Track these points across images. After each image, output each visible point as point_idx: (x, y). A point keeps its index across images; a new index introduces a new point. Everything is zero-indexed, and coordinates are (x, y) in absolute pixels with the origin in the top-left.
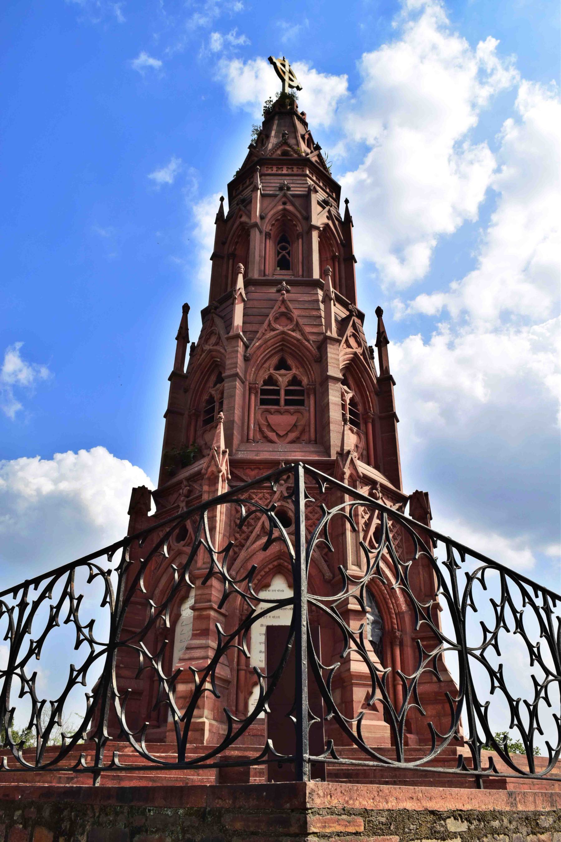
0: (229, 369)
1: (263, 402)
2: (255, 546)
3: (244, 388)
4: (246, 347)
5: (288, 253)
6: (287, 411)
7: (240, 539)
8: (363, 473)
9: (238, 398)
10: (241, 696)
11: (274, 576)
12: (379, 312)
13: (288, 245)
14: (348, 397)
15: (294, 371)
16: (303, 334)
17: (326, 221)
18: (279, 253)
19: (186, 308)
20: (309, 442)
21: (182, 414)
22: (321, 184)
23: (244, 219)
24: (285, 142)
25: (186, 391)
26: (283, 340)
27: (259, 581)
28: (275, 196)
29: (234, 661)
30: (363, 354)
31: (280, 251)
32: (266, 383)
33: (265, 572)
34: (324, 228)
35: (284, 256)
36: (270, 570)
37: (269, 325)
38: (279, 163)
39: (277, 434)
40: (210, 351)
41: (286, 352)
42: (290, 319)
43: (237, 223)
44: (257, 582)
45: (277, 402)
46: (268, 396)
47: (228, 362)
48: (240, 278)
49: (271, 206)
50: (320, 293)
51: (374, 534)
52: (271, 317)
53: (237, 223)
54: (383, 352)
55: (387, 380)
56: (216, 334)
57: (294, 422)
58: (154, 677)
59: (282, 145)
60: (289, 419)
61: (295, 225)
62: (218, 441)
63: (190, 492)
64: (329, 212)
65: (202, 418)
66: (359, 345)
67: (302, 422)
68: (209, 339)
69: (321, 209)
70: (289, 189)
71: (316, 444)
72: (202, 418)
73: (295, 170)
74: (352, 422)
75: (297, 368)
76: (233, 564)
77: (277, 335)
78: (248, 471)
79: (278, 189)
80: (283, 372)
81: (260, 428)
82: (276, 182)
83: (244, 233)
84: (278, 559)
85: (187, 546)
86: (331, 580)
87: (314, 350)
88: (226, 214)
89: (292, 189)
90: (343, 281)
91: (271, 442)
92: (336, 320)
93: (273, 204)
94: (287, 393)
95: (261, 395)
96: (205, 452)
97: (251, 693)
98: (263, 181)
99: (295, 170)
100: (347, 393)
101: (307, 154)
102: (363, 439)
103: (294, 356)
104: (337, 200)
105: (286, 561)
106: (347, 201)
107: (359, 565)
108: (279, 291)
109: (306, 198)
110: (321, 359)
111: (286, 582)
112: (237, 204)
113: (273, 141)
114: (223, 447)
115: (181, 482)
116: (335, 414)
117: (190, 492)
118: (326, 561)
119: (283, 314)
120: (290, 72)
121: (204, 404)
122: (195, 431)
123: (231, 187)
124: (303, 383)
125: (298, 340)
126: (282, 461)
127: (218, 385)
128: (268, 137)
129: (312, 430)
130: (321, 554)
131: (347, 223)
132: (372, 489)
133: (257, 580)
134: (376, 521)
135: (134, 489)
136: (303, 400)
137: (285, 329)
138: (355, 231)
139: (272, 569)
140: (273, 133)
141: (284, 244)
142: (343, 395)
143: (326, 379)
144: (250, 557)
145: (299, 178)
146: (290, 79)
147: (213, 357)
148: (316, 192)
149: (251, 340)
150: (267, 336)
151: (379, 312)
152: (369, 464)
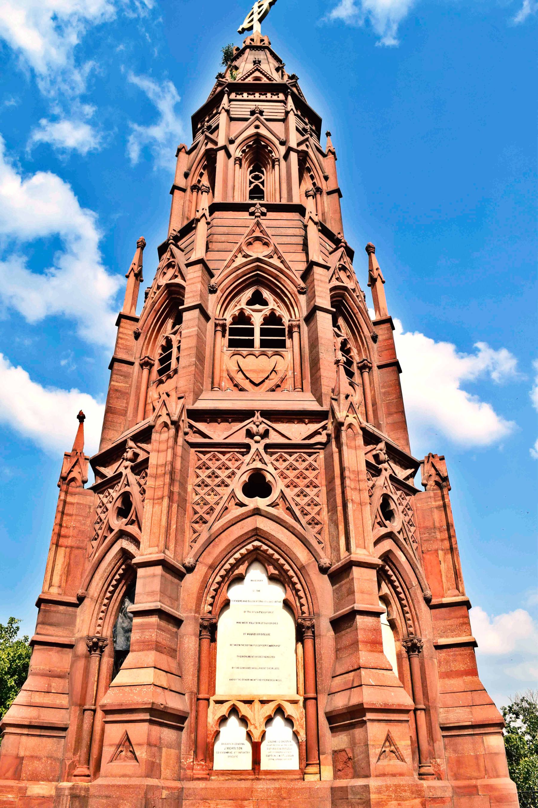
0: (188, 298)
1: (232, 344)
5: (262, 183)
6: (263, 354)
7: (201, 513)
13: (261, 175)
15: (271, 306)
18: (251, 183)
28: (246, 120)
31: (253, 180)
35: (257, 185)
36: (243, 556)
38: (251, 88)
39: (251, 382)
40: (168, 286)
45: (250, 344)
52: (242, 240)
56: (173, 267)
58: (85, 705)
59: (253, 72)
61: (271, 152)
70: (261, 113)
71: (303, 391)
72: (157, 367)
79: (249, 113)
80: (257, 307)
85: (131, 524)
91: (242, 390)
94: (263, 332)
95: (229, 335)
98: (231, 106)
100: (338, 336)
108: (252, 214)
112: (203, 133)
115: (125, 442)
119: (257, 239)
121: (160, 351)
124: (283, 320)
126: (258, 411)
136: (285, 340)
141: (257, 173)
151: (370, 250)
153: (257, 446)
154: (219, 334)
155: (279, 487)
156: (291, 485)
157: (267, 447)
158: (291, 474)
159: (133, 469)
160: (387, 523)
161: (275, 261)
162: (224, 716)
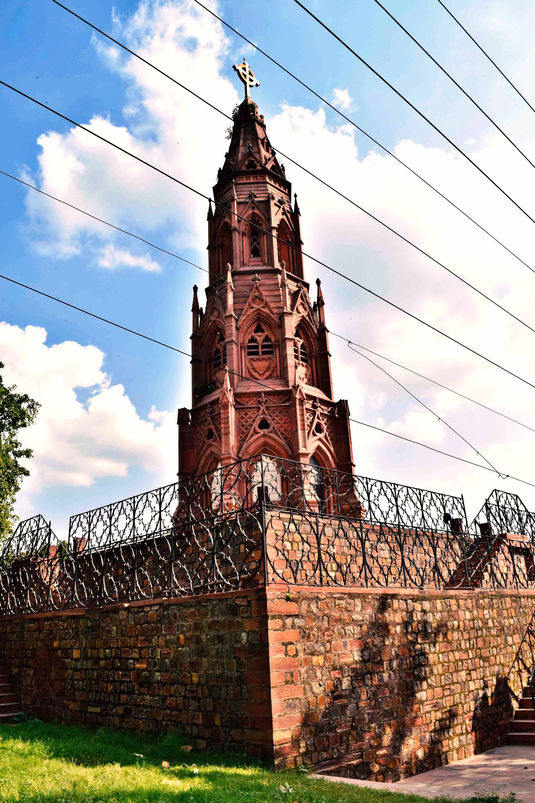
3: (238, 347)
4: (237, 321)
5: (258, 244)
6: (264, 359)
8: (306, 395)
9: (235, 357)
12: (318, 282)
14: (299, 345)
15: (266, 333)
16: (270, 310)
17: (281, 217)
18: (252, 244)
19: (195, 288)
20: (277, 378)
21: (202, 361)
22: (277, 186)
23: (227, 220)
24: (250, 154)
25: (202, 346)
26: (258, 314)
28: (247, 203)
30: (308, 315)
32: (250, 341)
34: (281, 222)
37: (249, 305)
38: (247, 174)
40: (215, 321)
41: (261, 322)
42: (262, 300)
43: (222, 222)
46: (252, 350)
47: (227, 333)
48: (229, 273)
49: (244, 212)
50: (279, 277)
51: (316, 428)
53: (222, 222)
54: (321, 311)
55: (323, 330)
57: (267, 366)
60: (265, 364)
62: (226, 384)
63: (212, 411)
64: (284, 209)
65: (213, 364)
66: (305, 309)
67: (273, 365)
68: (213, 312)
69: (278, 208)
70: (255, 196)
73: (259, 178)
74: (302, 359)
75: (268, 331)
77: (256, 311)
78: (244, 399)
80: (259, 334)
81: (249, 371)
82: (246, 190)
83: (228, 231)
85: (215, 441)
87: (277, 320)
88: (214, 212)
89: (258, 195)
90: (295, 259)
92: (290, 293)
93: (246, 209)
94: (263, 347)
96: (218, 385)
98: (238, 190)
99: (259, 178)
101: (266, 163)
102: (310, 370)
103: (265, 323)
104: (289, 194)
106: (296, 196)
107: (305, 447)
109: (266, 204)
110: (281, 326)
113: (242, 150)
114: (229, 387)
115: (206, 405)
116: (291, 361)
117: (212, 411)
119: (256, 297)
120: (250, 74)
122: (210, 371)
123: (215, 189)
125: (267, 314)
127: (221, 343)
128: (238, 145)
129: (279, 370)
131: (295, 214)
132: (314, 402)
134: (316, 420)
135: (179, 410)
137: (259, 307)
138: (301, 219)
140: (241, 141)
142: (295, 345)
143: (285, 340)
145: (262, 185)
146: (251, 80)
147: (217, 325)
148: (273, 199)
149: (239, 315)
150: (248, 313)
151: (318, 282)
152: (313, 386)
153: (263, 408)
154: (243, 352)
155: (273, 424)
156: (278, 423)
157: (267, 408)
158: (277, 419)
159: (212, 418)
160: (318, 434)
161: (266, 310)
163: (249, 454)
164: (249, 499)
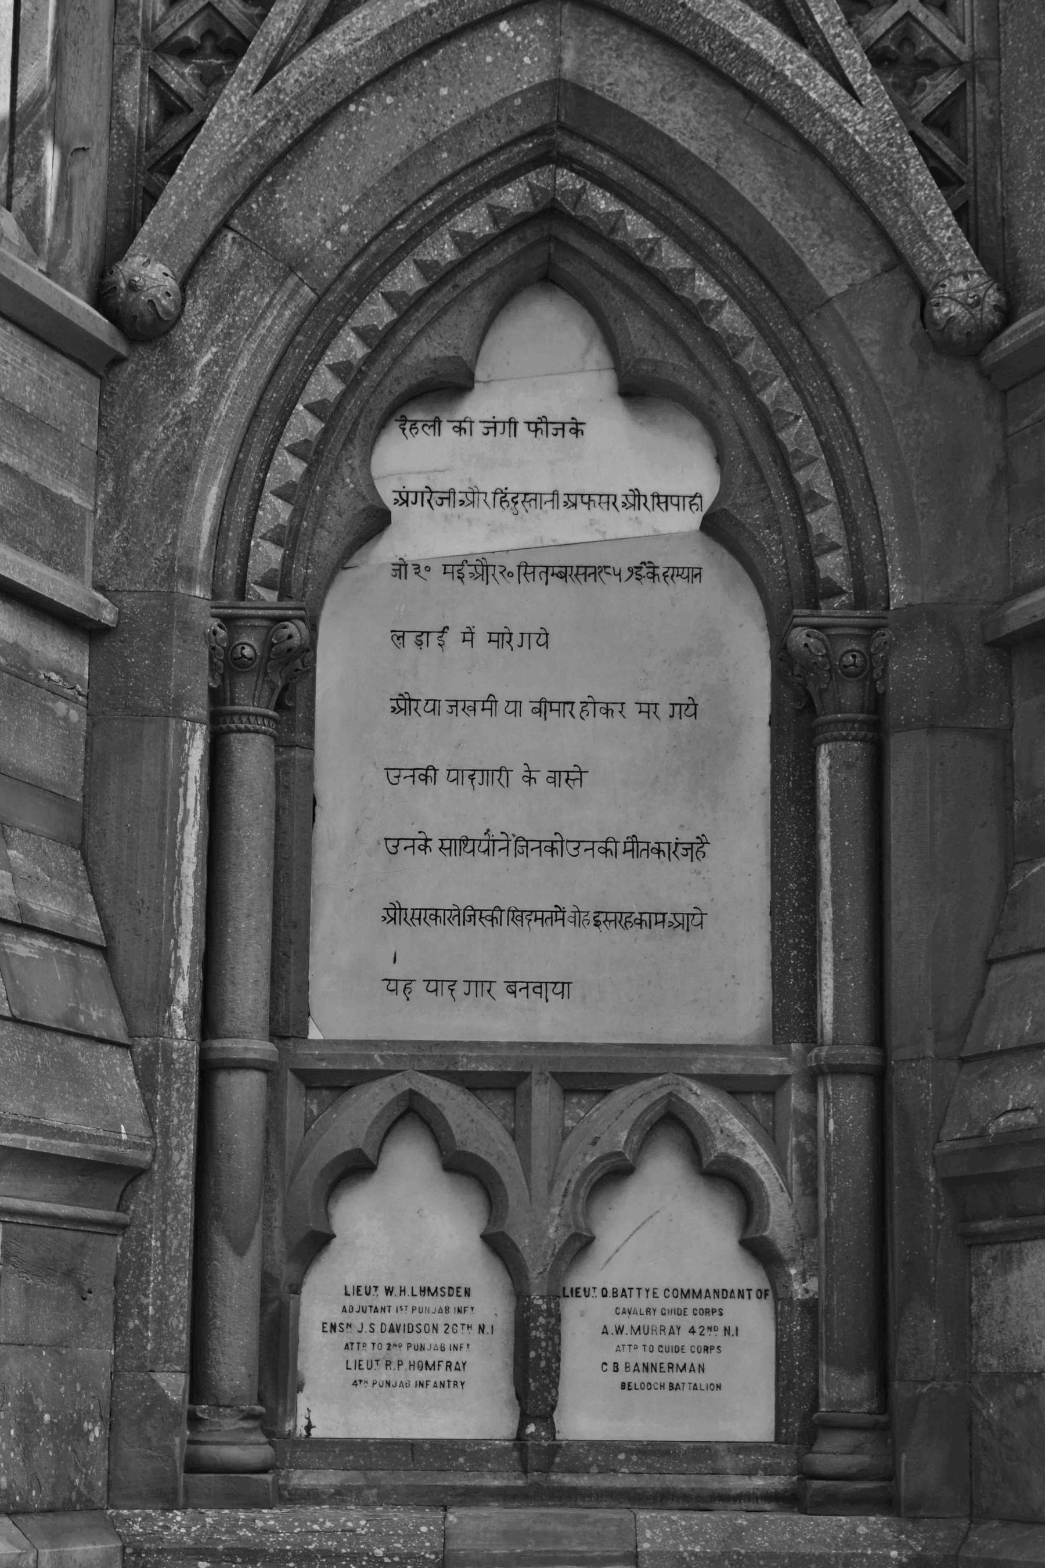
2: (337, 41)
10: (237, 1277)
11: (502, 303)
27: (378, 341)
29: (170, 1000)
33: (423, 267)
36: (473, 250)
44: (360, 351)
76: (151, 197)
84: (537, 162)
86: (996, 332)
97: (319, 1241)
105: (602, 181)
111: (598, 354)
118: (944, 177)
130: (904, 113)
133: (362, 334)
139: (488, 244)
144: (301, 142)
162: (359, 1152)
163: (293, 265)
164: (247, 993)
